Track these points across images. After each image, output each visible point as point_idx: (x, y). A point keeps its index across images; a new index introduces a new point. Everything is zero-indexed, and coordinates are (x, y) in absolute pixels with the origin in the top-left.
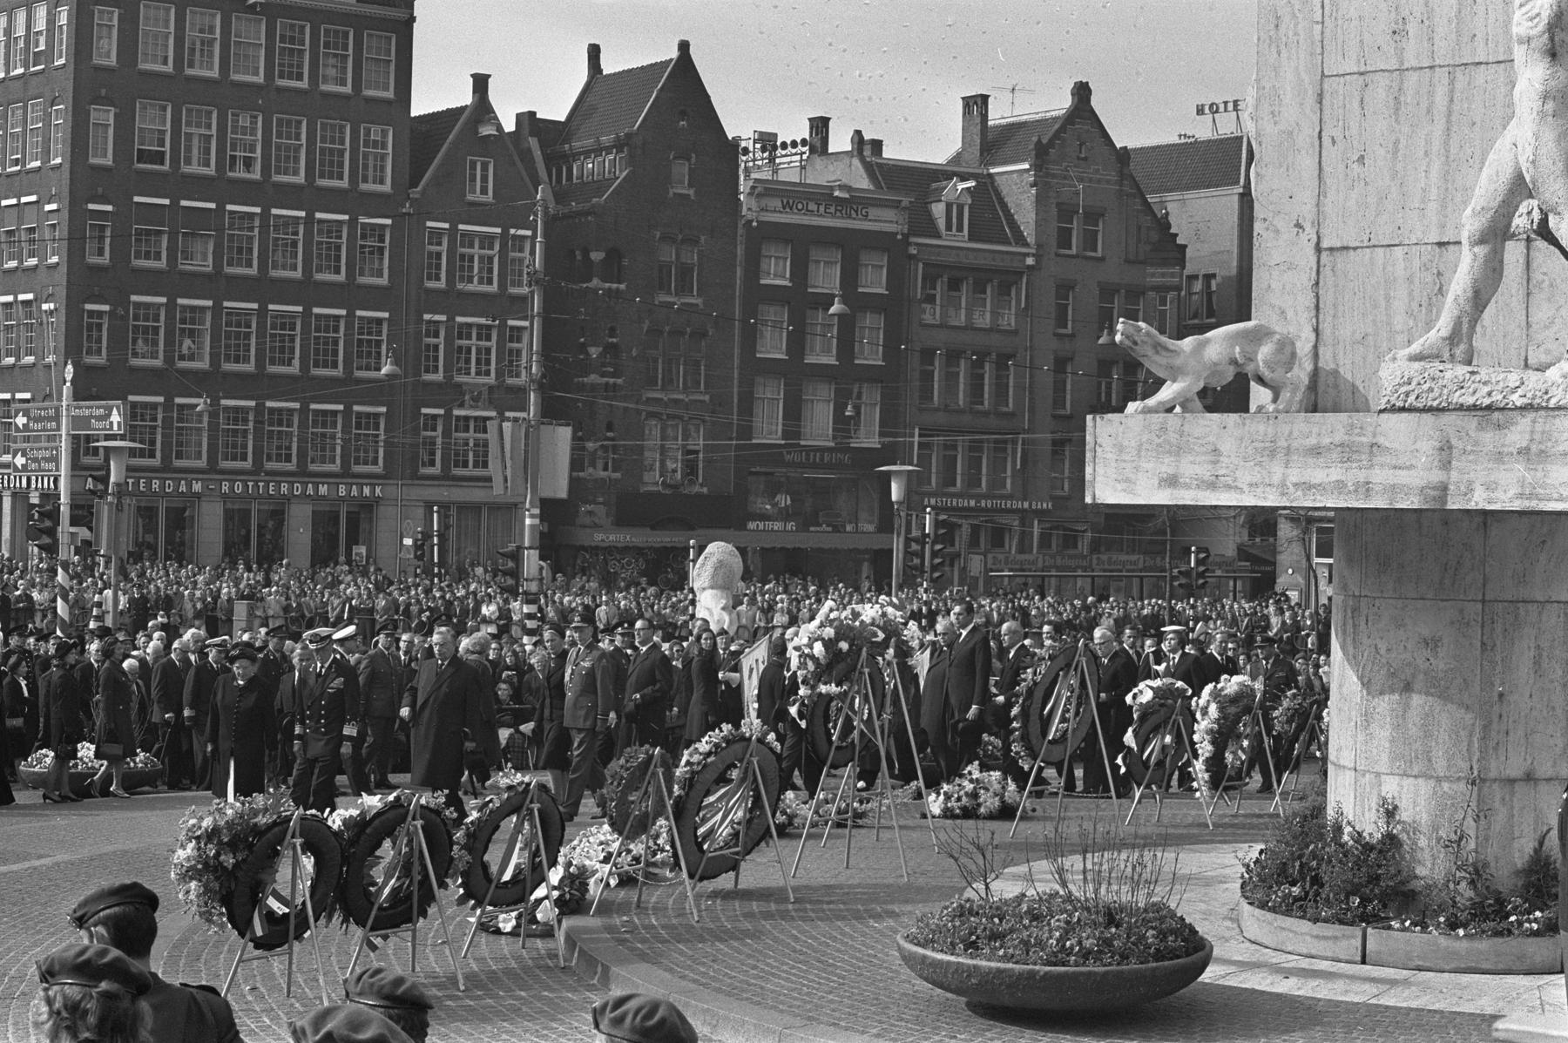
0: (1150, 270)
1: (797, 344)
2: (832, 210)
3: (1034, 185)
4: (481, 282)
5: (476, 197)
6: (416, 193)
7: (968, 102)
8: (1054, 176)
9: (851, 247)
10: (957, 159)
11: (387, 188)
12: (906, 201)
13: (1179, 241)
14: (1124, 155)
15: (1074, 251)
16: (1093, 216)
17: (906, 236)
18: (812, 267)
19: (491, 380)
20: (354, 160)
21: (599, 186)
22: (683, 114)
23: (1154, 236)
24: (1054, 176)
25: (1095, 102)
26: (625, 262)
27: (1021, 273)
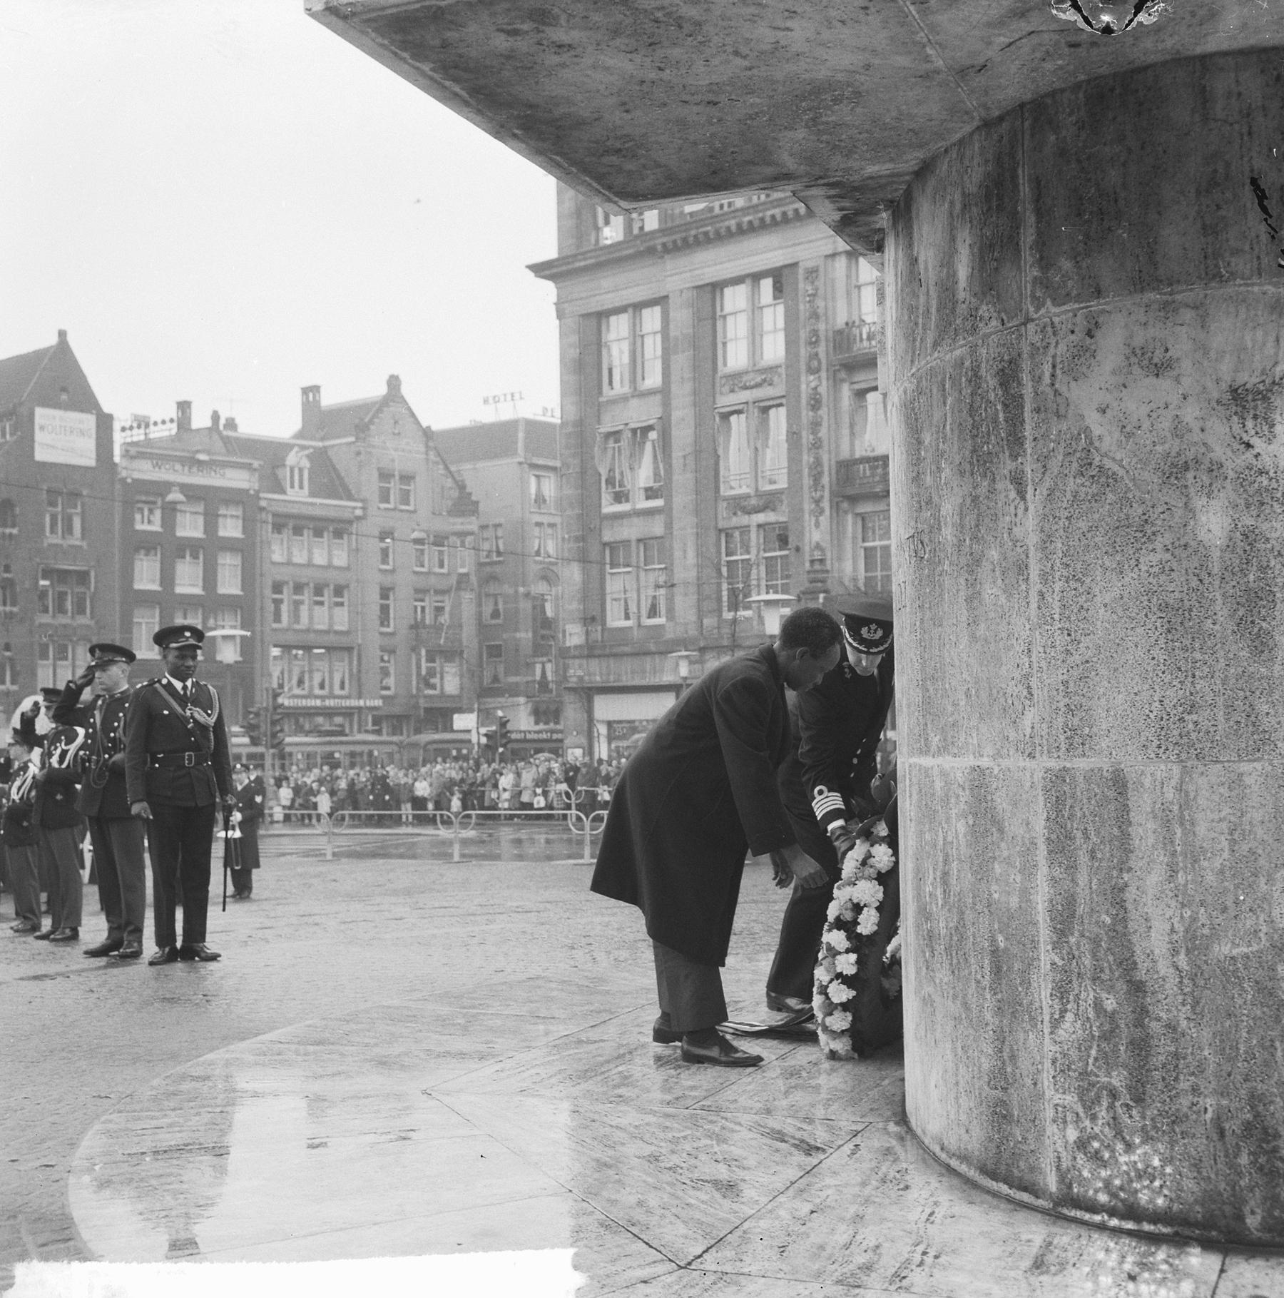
0: (451, 520)
1: (167, 578)
2: (195, 469)
3: (358, 453)
7: (306, 391)
8: (374, 447)
9: (211, 501)
10: (300, 435)
13: (474, 498)
14: (427, 434)
15: (391, 506)
16: (407, 478)
17: (257, 492)
18: (179, 517)
22: (64, 390)
25: (406, 391)
26: (17, 510)
27: (350, 522)
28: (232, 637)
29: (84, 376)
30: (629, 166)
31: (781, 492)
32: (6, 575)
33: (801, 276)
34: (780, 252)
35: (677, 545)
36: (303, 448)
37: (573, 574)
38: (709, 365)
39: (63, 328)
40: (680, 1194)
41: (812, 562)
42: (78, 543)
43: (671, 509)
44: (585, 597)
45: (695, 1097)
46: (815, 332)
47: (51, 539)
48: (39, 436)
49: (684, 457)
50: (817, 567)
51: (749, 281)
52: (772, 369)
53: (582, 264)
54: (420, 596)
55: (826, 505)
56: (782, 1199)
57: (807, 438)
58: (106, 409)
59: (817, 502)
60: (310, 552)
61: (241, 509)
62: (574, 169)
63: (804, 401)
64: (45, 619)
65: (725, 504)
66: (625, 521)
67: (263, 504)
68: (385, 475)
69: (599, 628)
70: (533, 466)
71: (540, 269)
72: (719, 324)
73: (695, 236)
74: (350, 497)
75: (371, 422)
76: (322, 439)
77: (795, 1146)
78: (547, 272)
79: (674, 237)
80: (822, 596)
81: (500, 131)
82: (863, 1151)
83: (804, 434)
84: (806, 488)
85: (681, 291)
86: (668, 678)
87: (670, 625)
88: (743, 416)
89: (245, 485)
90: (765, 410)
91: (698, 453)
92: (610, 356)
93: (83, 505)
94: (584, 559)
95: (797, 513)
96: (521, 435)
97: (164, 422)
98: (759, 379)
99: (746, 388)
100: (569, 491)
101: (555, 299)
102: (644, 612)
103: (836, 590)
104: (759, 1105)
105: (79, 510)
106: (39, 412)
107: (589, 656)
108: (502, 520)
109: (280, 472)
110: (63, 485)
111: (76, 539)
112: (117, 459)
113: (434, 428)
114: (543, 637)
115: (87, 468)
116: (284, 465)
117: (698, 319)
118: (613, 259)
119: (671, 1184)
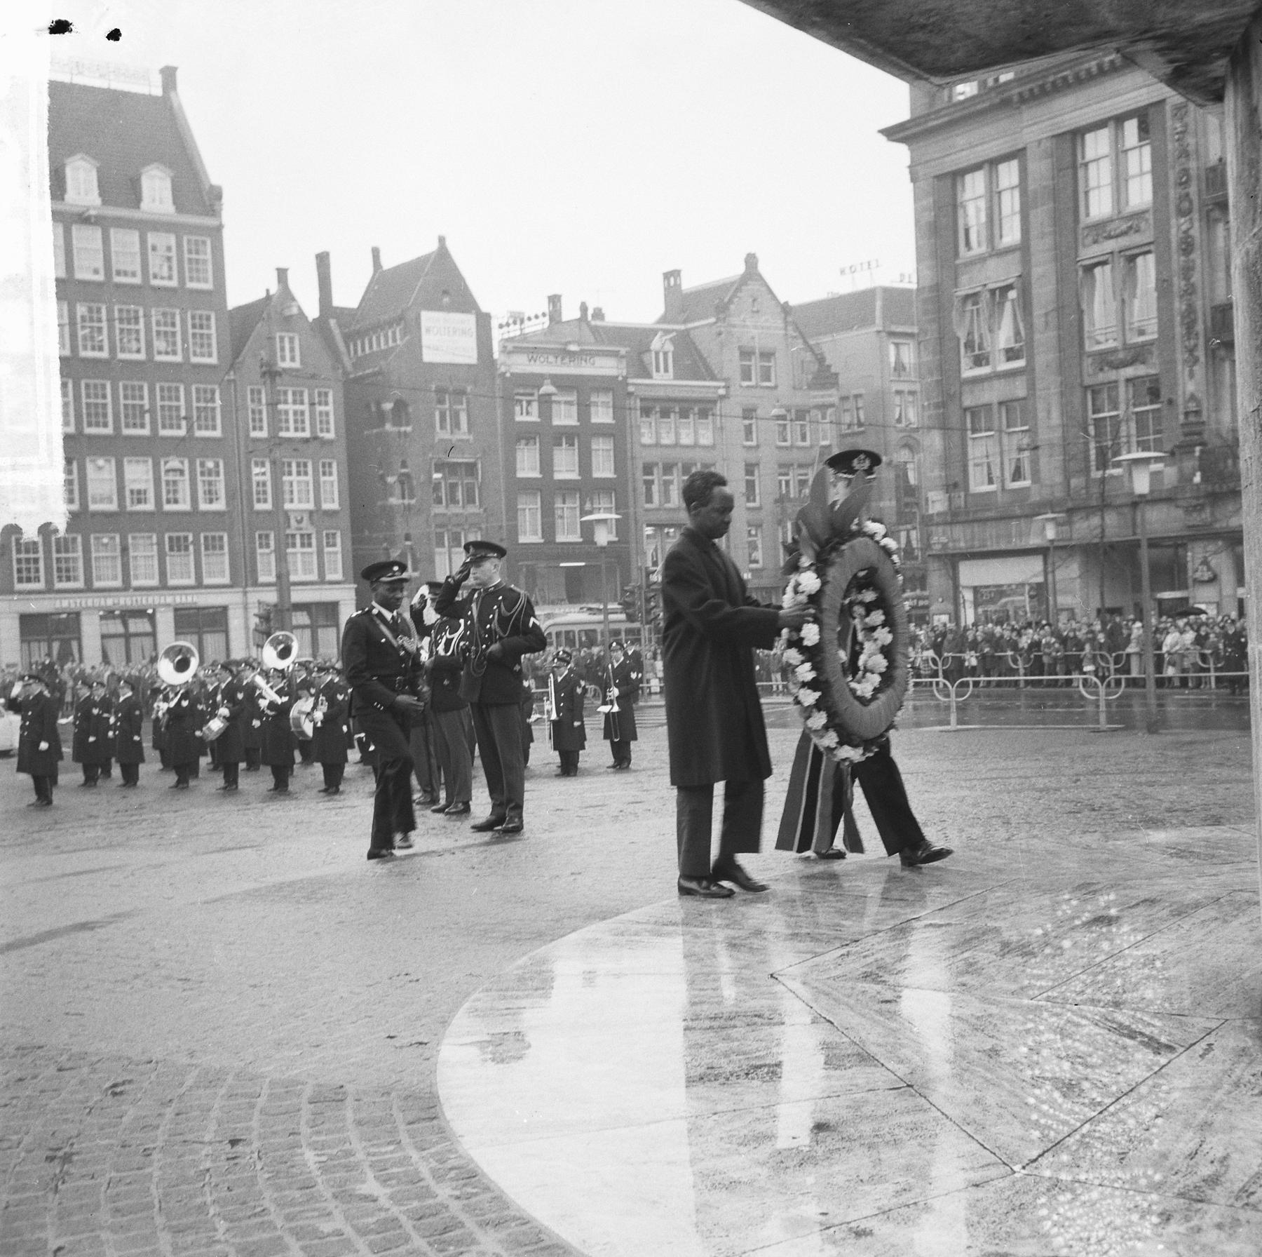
1: (547, 465)
2: (567, 360)
3: (720, 334)
4: (296, 430)
5: (287, 364)
7: (667, 276)
8: (734, 326)
9: (581, 389)
10: (663, 319)
12: (623, 351)
13: (833, 370)
14: (786, 309)
16: (767, 355)
17: (625, 378)
18: (554, 406)
19: (311, 506)
20: (184, 341)
21: (385, 354)
22: (445, 292)
23: (815, 367)
24: (734, 326)
26: (410, 410)
27: (715, 402)
28: (604, 521)
29: (461, 279)
30: (937, 41)
31: (1151, 343)
32: (403, 471)
33: (1169, 114)
34: (1144, 90)
35: (1041, 406)
36: (667, 332)
37: (934, 441)
38: (1069, 219)
39: (443, 233)
40: (1018, 1091)
41: (1187, 414)
42: (464, 437)
43: (1033, 370)
44: (946, 462)
45: (1041, 987)
46: (1186, 171)
47: (442, 435)
48: (426, 339)
49: (1046, 314)
50: (1192, 419)
51: (1112, 124)
52: (1139, 215)
53: (935, 123)
54: (782, 471)
55: (1200, 353)
56: (1125, 1100)
57: (1178, 284)
59: (1191, 351)
60: (677, 434)
61: (610, 395)
62: (879, 51)
63: (1174, 245)
64: (440, 509)
65: (1090, 360)
66: (986, 384)
67: (631, 389)
68: (746, 354)
69: (962, 494)
70: (892, 334)
71: (893, 133)
72: (1081, 173)
73: (1054, 83)
74: (713, 378)
75: (730, 301)
76: (685, 322)
77: (1142, 1043)
78: (901, 135)
79: (1028, 87)
80: (1198, 449)
81: (798, 20)
82: (1217, 1051)
83: (1175, 280)
84: (1178, 337)
85: (1040, 142)
86: (1034, 541)
87: (1035, 488)
88: (1108, 268)
89: (613, 372)
90: (1132, 259)
91: (1060, 309)
92: (966, 216)
93: (468, 402)
94: (944, 427)
95: (1170, 364)
96: (879, 304)
97: (537, 317)
98: (1124, 227)
99: (1110, 237)
100: (927, 358)
101: (908, 162)
102: (1008, 475)
103: (1214, 442)
104: (1109, 998)
105: (464, 406)
106: (428, 318)
108: (862, 391)
109: (646, 358)
110: (451, 385)
111: (463, 433)
112: (496, 355)
113: (793, 302)
114: (907, 505)
115: (470, 366)
116: (649, 350)
117: (1058, 170)
118: (969, 115)
119: (1011, 1082)
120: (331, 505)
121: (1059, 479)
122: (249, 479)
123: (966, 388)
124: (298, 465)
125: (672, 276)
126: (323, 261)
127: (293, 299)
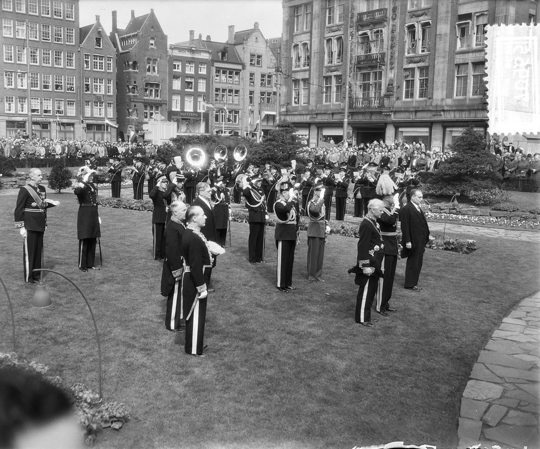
4: (100, 68)
6: (81, 45)
11: (74, 44)
14: (266, 41)
16: (259, 57)
18: (187, 68)
25: (260, 28)
39: (152, 8)
42: (156, 75)
58: (165, 33)
68: (252, 55)
94: (286, 84)
107: (287, 115)
111: (156, 74)
120: (111, 94)
121: (314, 104)
122: (83, 83)
123: (293, 74)
124: (100, 80)
125: (231, 27)
126: (114, 14)
127: (101, 26)
